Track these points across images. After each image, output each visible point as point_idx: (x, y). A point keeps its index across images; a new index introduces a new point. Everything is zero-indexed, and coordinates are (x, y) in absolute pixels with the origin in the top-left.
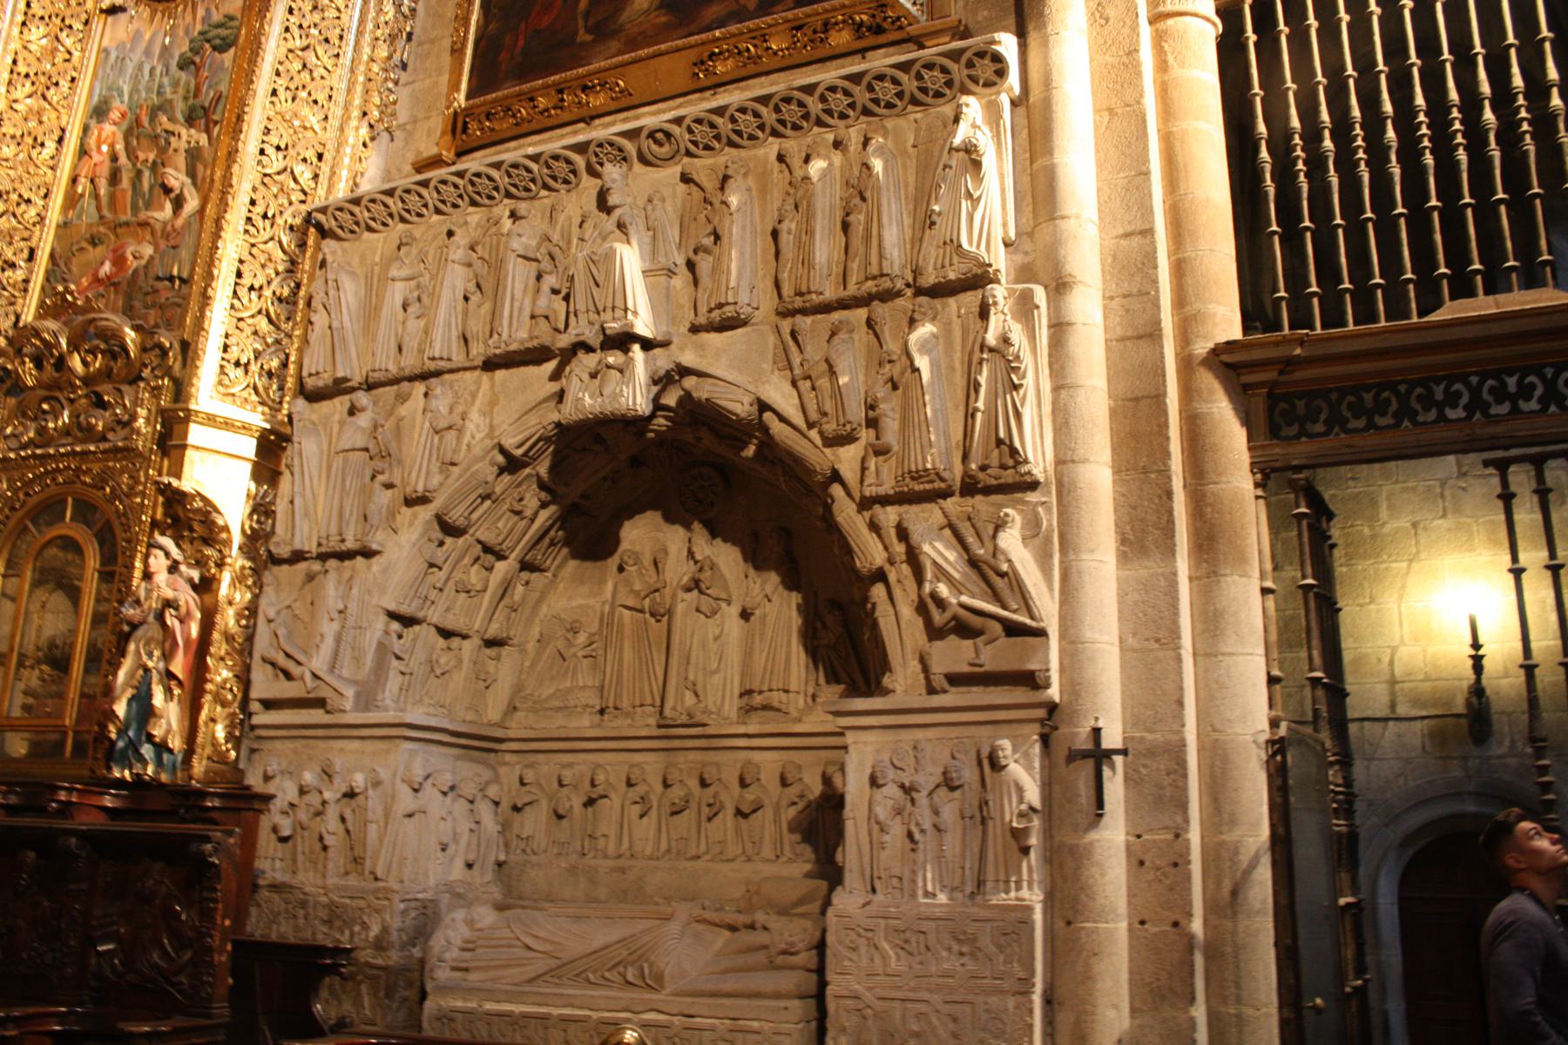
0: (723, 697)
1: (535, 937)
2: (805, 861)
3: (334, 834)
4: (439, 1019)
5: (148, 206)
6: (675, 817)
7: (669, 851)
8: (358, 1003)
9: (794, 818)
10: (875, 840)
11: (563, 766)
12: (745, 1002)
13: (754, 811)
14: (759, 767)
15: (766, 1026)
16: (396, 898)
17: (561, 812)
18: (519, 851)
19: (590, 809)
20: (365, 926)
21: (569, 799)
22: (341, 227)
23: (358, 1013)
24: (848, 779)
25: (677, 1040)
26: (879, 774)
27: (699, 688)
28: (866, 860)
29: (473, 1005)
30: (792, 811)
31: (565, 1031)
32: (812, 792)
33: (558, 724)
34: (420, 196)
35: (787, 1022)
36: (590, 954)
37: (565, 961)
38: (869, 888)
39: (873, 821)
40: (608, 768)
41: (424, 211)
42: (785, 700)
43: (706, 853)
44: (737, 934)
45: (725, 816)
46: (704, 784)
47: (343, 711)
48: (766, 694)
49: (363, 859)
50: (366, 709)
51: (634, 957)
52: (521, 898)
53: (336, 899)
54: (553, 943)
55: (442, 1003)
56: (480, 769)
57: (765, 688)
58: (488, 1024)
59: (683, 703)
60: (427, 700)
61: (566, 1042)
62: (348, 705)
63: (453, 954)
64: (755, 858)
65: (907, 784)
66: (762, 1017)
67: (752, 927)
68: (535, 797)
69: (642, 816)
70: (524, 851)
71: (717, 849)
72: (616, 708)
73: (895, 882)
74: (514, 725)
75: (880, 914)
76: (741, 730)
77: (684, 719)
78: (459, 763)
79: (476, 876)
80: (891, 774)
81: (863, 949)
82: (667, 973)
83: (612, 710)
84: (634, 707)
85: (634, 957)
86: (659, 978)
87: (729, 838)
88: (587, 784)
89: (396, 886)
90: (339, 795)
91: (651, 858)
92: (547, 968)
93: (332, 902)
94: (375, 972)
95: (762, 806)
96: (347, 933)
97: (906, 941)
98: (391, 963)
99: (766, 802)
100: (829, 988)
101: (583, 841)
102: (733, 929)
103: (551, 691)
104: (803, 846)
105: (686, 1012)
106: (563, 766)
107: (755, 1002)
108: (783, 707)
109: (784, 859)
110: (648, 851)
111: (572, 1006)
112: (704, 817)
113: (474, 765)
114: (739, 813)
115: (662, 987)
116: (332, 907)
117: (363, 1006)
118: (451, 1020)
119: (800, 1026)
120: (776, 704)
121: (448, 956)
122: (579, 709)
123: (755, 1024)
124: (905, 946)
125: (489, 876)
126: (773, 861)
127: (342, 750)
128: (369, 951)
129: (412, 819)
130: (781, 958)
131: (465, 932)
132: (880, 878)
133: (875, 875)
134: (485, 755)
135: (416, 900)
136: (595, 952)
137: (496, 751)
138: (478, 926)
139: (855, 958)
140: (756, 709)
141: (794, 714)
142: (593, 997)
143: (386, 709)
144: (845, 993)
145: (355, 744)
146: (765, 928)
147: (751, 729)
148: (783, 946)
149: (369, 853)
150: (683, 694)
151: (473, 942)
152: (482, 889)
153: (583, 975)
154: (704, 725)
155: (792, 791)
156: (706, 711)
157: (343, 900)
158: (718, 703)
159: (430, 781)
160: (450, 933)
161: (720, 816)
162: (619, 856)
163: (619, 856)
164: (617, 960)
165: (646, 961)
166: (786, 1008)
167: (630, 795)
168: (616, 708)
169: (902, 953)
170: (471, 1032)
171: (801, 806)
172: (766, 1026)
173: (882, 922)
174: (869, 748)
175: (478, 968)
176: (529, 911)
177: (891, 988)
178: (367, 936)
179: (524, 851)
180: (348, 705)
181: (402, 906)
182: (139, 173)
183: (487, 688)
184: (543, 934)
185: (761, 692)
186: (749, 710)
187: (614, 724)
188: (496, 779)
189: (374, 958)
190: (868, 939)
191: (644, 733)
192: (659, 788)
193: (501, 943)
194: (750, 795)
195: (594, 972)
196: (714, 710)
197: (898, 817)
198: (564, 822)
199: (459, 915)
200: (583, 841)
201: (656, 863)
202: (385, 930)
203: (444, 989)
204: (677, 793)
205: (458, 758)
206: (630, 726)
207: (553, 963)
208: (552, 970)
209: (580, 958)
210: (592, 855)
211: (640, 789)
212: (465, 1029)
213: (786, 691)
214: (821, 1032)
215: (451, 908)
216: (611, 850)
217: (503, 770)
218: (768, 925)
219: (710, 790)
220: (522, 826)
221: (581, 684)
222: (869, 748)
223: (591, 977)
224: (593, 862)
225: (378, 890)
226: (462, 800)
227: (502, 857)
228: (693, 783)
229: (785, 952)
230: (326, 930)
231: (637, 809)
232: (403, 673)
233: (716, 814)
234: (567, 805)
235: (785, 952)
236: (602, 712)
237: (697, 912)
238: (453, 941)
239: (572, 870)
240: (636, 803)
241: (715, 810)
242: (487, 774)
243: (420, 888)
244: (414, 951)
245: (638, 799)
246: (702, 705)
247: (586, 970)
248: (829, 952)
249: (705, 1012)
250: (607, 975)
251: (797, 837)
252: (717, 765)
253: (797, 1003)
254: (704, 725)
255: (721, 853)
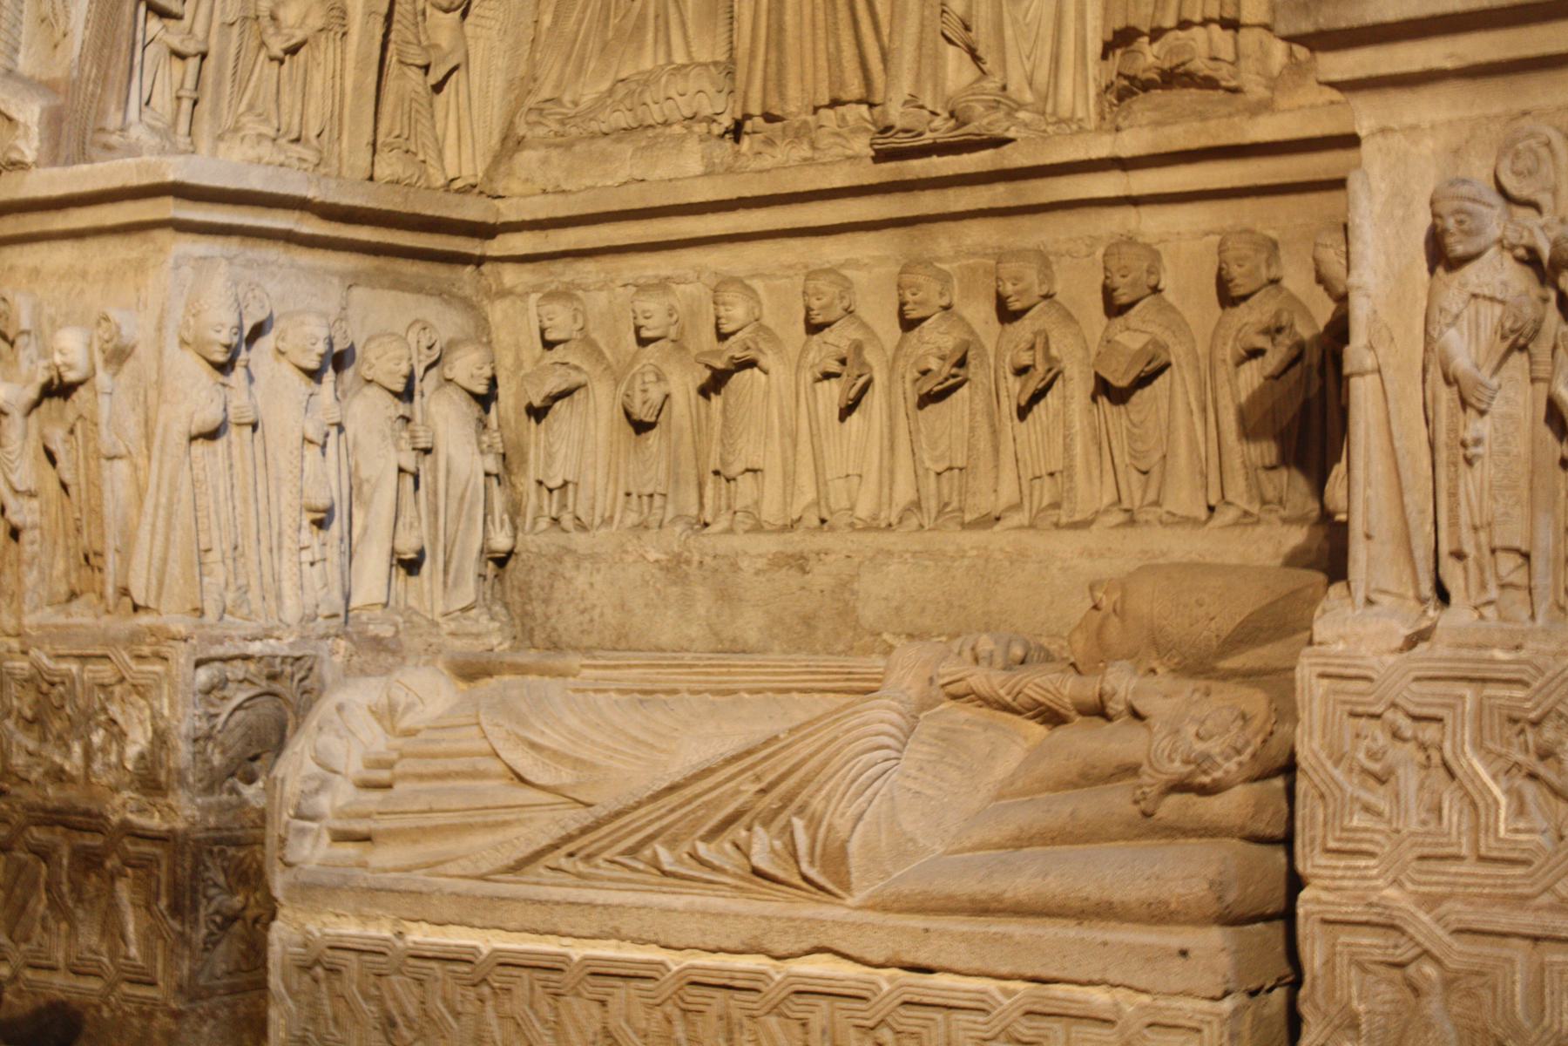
0: (1056, 60)
1: (533, 746)
2: (1285, 521)
3: (32, 495)
4: (306, 968)
6: (931, 408)
7: (917, 505)
8: (112, 930)
9: (1255, 398)
10: (1442, 438)
11: (642, 288)
12: (1069, 931)
13: (1144, 381)
14: (1156, 255)
15: (1131, 1004)
16: (181, 656)
17: (642, 413)
18: (544, 523)
19: (716, 401)
20: (120, 736)
21: (660, 378)
23: (113, 954)
24: (1356, 247)
25: (885, 1035)
26: (1451, 223)
27: (982, 36)
28: (1418, 499)
29: (381, 931)
30: (1251, 377)
31: (603, 1003)
32: (1309, 317)
33: (622, 176)
35: (1187, 994)
36: (655, 797)
37: (600, 812)
38: (1427, 588)
39: (1435, 374)
40: (757, 284)
42: (1227, 53)
43: (1016, 507)
44: (1060, 732)
45: (1066, 402)
46: (1007, 314)
47: (18, 165)
48: (1170, 36)
49: (99, 554)
50: (83, 156)
51: (772, 800)
52: (555, 646)
53: (51, 664)
54: (578, 763)
55: (311, 927)
56: (429, 309)
57: (1169, 21)
58: (420, 982)
59: (938, 84)
60: (252, 126)
61: (607, 1033)
62: (29, 147)
63: (338, 799)
64: (1151, 514)
65: (1546, 251)
66: (1113, 976)
67: (1099, 711)
68: (575, 378)
69: (846, 412)
70: (556, 520)
71: (1045, 493)
72: (769, 118)
73: (1508, 563)
74: (516, 186)
75: (1464, 669)
76: (1101, 148)
77: (941, 129)
78: (359, 293)
79: (426, 588)
80: (1494, 221)
81: (1409, 779)
82: (853, 847)
83: (759, 121)
84: (816, 110)
85: (772, 800)
86: (835, 859)
87: (1079, 462)
88: (708, 338)
89: (179, 626)
90: (32, 393)
91: (870, 527)
92: (557, 833)
93: (39, 671)
94: (146, 848)
95: (1167, 365)
96: (77, 749)
97: (1545, 755)
98: (180, 825)
99: (1177, 353)
100: (1304, 895)
101: (701, 486)
102: (1052, 717)
103: (605, 86)
104: (1283, 475)
105: (909, 959)
106: (642, 288)
107: (1095, 933)
108: (1223, 73)
109: (1230, 515)
110: (864, 510)
111: (616, 935)
112: (1008, 407)
113: (408, 298)
114: (1104, 390)
115: (847, 887)
116: (40, 682)
117: (123, 937)
118: (333, 971)
119: (1227, 1005)
120: (1200, 66)
121: (324, 802)
122: (677, 129)
123: (1099, 998)
124: (1541, 769)
125: (468, 591)
126: (1193, 522)
127: (35, 273)
128: (126, 794)
129: (220, 444)
130: (1175, 799)
131: (376, 740)
132: (1459, 555)
133: (1444, 548)
134: (442, 271)
135: (246, 658)
136: (672, 789)
137: (479, 261)
138: (406, 722)
139: (1384, 806)
140: (1147, 86)
141: (1256, 90)
142: (667, 911)
143: (133, 150)
144: (1357, 912)
145: (62, 255)
146: (1136, 715)
147: (1131, 143)
148: (1178, 768)
149: (112, 541)
150: (938, 57)
151: (389, 765)
152: (447, 626)
153: (647, 853)
154: (999, 142)
155: (1251, 317)
156: (1003, 100)
157: (64, 666)
158: (1042, 76)
159: (266, 343)
160: (328, 740)
161: (1051, 399)
162: (791, 526)
163: (791, 526)
164: (729, 809)
165: (800, 811)
166: (1184, 953)
167: (812, 356)
168: (769, 118)
169: (1530, 790)
170: (380, 1000)
171: (1274, 359)
172: (1131, 1004)
173: (1468, 691)
174: (1428, 145)
175: (393, 834)
176: (532, 678)
177: (1492, 899)
178: (121, 754)
179: (556, 520)
180: (29, 147)
181: (203, 675)
183: (438, 88)
184: (551, 739)
185: (1156, 34)
186: (1128, 89)
187: (767, 162)
188: (482, 333)
189: (141, 811)
190: (1423, 747)
191: (839, 178)
192: (889, 329)
193: (453, 765)
194: (1133, 335)
195: (672, 844)
196: (1028, 97)
197: (1518, 360)
198: (653, 435)
199: (361, 695)
200: (701, 486)
201: (886, 540)
202: (160, 739)
203: (312, 891)
204: (936, 339)
205: (353, 281)
206: (809, 162)
207: (573, 818)
208: (569, 838)
209: (639, 805)
210: (723, 523)
211: (839, 338)
212: (367, 997)
213: (1232, 25)
214: (1294, 1023)
215: (350, 671)
216: (771, 511)
217: (497, 312)
218: (1140, 706)
219: (1023, 329)
220: (550, 456)
221: (679, 58)
222: (1428, 145)
223: (666, 858)
224: (725, 544)
225: (135, 637)
226: (373, 391)
227: (501, 541)
228: (980, 314)
229: (1181, 786)
230: (32, 745)
231: (833, 393)
232: (182, 56)
233: (1038, 396)
234: (655, 395)
235: (1181, 786)
236: (737, 132)
237: (949, 670)
238: (339, 764)
239: (675, 567)
240: (827, 376)
241: (1034, 383)
242: (447, 323)
243: (251, 628)
244: (249, 792)
245: (834, 367)
246: (991, 85)
247: (651, 838)
248: (1302, 785)
249: (963, 960)
250: (702, 849)
251: (1266, 451)
252: (1044, 260)
253: (1216, 936)
254: (999, 142)
255: (1056, 505)
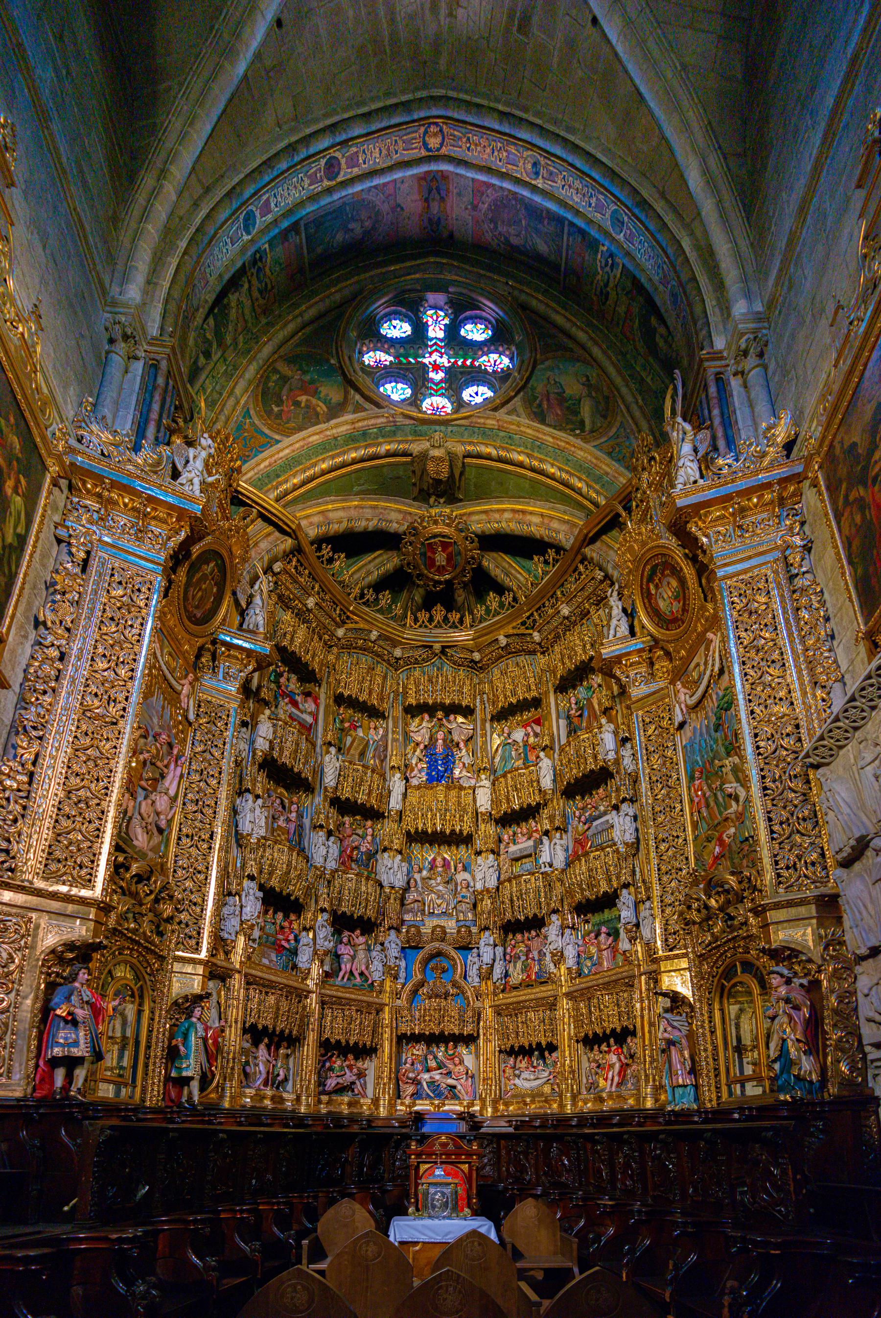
5: (726, 809)
22: (823, 758)
34: (855, 708)
41: (865, 714)
182: (715, 795)
